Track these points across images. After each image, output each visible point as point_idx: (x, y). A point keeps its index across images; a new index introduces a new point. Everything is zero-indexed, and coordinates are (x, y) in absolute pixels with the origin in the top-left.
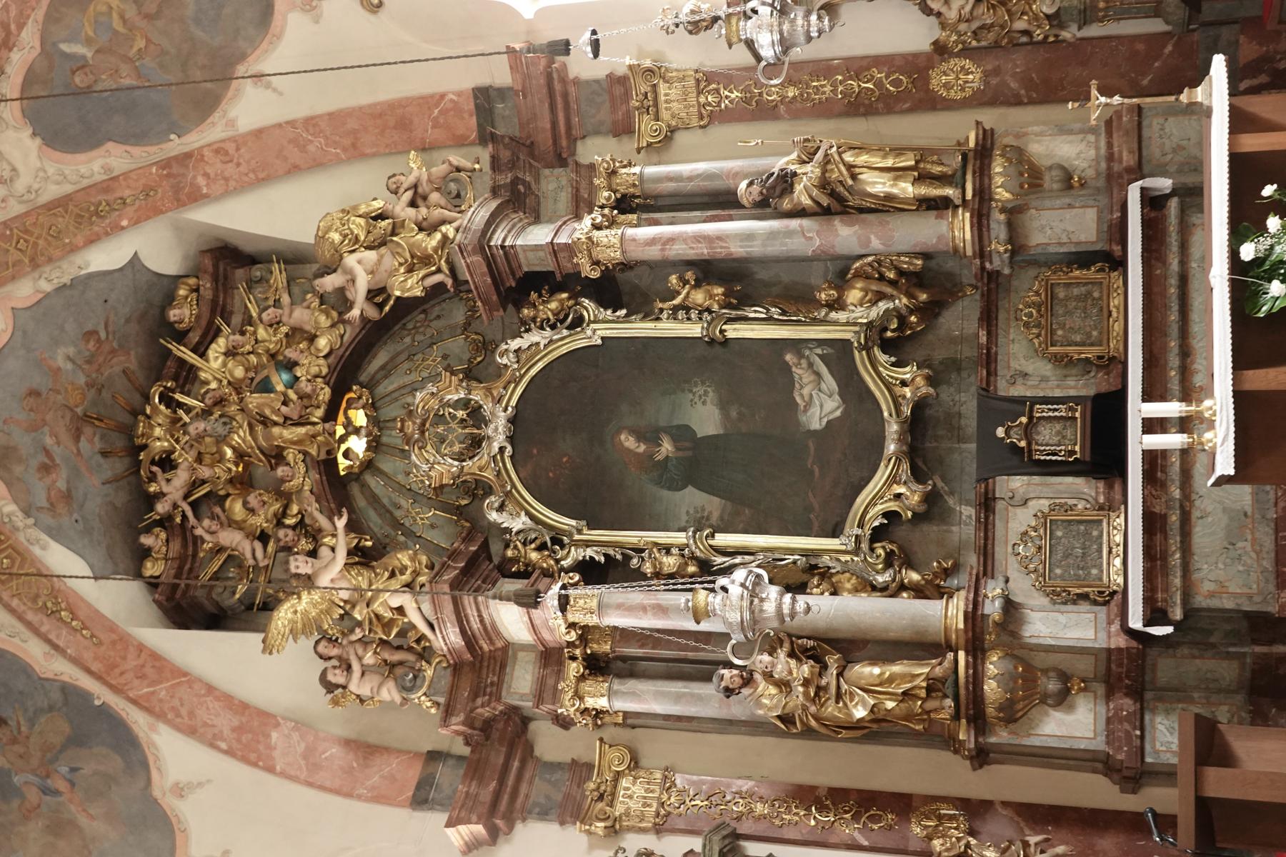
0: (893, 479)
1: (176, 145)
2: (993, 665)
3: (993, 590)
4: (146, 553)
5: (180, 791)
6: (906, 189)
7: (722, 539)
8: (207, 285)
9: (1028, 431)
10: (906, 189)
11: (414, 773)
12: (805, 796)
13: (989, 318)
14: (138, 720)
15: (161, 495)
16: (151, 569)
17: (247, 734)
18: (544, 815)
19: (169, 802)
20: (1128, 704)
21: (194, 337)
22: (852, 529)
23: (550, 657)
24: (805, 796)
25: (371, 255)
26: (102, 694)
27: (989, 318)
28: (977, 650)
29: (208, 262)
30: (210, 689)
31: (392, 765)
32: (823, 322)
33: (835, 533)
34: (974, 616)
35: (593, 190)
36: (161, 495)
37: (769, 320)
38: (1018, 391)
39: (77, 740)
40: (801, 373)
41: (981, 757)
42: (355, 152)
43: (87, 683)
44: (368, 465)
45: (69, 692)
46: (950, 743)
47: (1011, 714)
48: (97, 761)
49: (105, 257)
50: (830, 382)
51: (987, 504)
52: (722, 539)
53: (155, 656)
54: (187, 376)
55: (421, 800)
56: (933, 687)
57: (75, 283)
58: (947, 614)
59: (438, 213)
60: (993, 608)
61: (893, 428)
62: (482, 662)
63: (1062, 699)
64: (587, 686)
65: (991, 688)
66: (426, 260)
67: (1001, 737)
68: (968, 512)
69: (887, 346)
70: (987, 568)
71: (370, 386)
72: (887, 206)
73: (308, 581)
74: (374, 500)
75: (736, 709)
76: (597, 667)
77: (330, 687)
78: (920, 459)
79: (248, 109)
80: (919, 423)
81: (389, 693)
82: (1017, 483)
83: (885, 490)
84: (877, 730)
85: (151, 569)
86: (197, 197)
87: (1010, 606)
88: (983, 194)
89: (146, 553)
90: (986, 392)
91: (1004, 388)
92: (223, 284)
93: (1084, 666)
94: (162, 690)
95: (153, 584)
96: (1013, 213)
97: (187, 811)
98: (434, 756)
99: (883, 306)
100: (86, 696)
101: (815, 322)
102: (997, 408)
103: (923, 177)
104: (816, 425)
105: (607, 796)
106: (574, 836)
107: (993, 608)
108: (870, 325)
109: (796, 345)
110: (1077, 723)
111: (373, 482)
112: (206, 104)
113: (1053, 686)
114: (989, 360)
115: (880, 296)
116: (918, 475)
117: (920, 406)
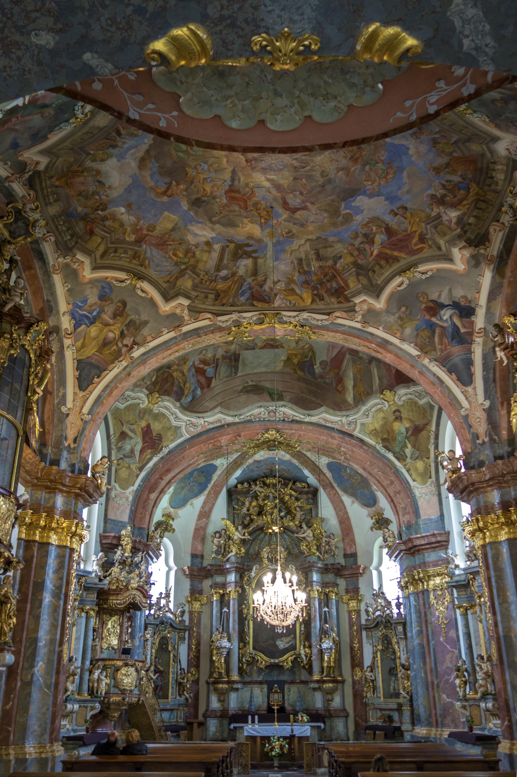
0: (266, 662)
1: (335, 485)
2: (225, 686)
3: (239, 686)
4: (242, 483)
5: (191, 504)
6: (325, 665)
7: (251, 623)
8: (306, 490)
9: (276, 692)
10: (325, 665)
11: (198, 553)
12: (198, 644)
13: (302, 682)
14: (206, 492)
15: (256, 485)
16: (239, 486)
17: (205, 514)
18: (191, 585)
19: (189, 503)
20: (219, 714)
21: (294, 487)
22: (254, 652)
23: (224, 586)
24: (198, 644)
25: (311, 535)
26: (210, 486)
27: (302, 682)
28: (228, 682)
29: (312, 489)
30: (214, 504)
31: (200, 548)
32: (300, 644)
33: (254, 648)
34: (234, 682)
35: (328, 588)
36: (256, 485)
37: (301, 630)
38: (286, 689)
39: (200, 484)
40: (289, 638)
41: (208, 683)
42: (341, 522)
43: (212, 482)
44: (266, 534)
45: (211, 480)
46: (211, 676)
47: (216, 690)
48: (196, 489)
49: (306, 472)
50: (287, 646)
51: (261, 683)
52: (251, 623)
53: (220, 493)
54: (286, 485)
55: (194, 556)
56: (220, 673)
57: (300, 469)
58: (235, 677)
59: (323, 549)
60: (235, 686)
61: (277, 661)
62: (223, 572)
63: (219, 701)
64: (218, 595)
65: (221, 686)
66: (310, 549)
67: (211, 688)
68: (261, 678)
69: (295, 659)
70: (245, 683)
71: (284, 532)
72: (322, 659)
73: (237, 529)
74: (259, 535)
75: (214, 629)
76: (222, 596)
77: (215, 533)
78: (271, 667)
79: (347, 500)
80: (279, 667)
81: (215, 548)
82: (266, 690)
83: (263, 660)
84: (212, 662)
85: (239, 486)
86: (325, 489)
87: (237, 690)
88: (324, 682)
89: (242, 483)
90: (285, 682)
91: (286, 686)
92: (307, 493)
93: (226, 705)
94: (213, 495)
95: (236, 486)
96: (319, 689)
97: (188, 507)
98: (202, 557)
99: (304, 658)
100: (209, 483)
101: (300, 641)
102: (282, 684)
103: (329, 667)
104: (277, 643)
105: (196, 600)
106: (187, 593)
107: (235, 686)
108: (300, 654)
109: (295, 637)
110: (215, 704)
111: (262, 535)
112: (346, 491)
113: (222, 699)
114: (292, 682)
115: (306, 657)
116: (267, 667)
117: (282, 667)
